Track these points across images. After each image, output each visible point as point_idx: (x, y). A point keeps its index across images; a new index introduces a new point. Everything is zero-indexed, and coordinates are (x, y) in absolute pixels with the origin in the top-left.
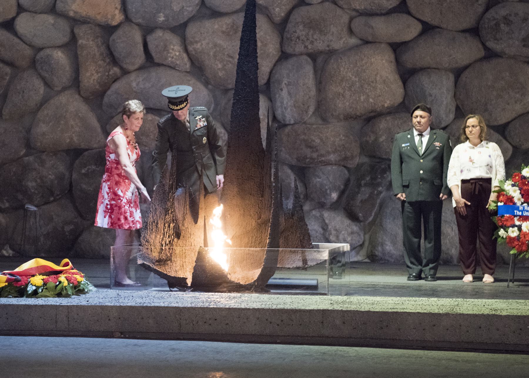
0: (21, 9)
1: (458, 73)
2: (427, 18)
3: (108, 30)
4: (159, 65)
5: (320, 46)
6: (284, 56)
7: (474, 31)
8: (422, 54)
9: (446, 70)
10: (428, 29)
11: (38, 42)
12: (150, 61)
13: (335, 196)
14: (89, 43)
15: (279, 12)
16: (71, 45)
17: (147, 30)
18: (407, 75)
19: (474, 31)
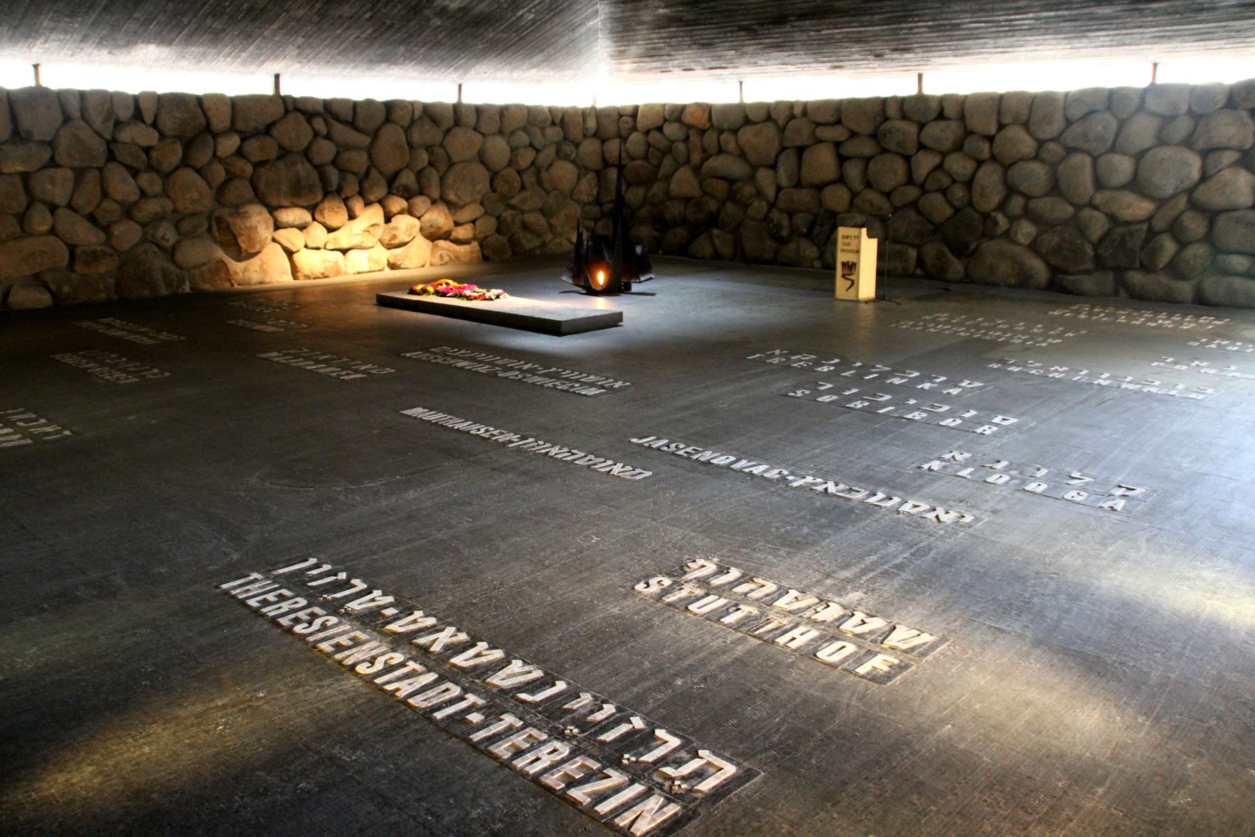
0: (665, 120)
1: (868, 159)
2: (853, 126)
3: (702, 132)
4: (726, 152)
5: (799, 143)
6: (784, 149)
7: (874, 136)
8: (847, 149)
9: (859, 158)
10: (853, 134)
11: (673, 138)
12: (721, 151)
13: (804, 230)
14: (694, 138)
15: (781, 122)
16: (686, 139)
17: (721, 131)
18: (842, 159)
19: (874, 136)
